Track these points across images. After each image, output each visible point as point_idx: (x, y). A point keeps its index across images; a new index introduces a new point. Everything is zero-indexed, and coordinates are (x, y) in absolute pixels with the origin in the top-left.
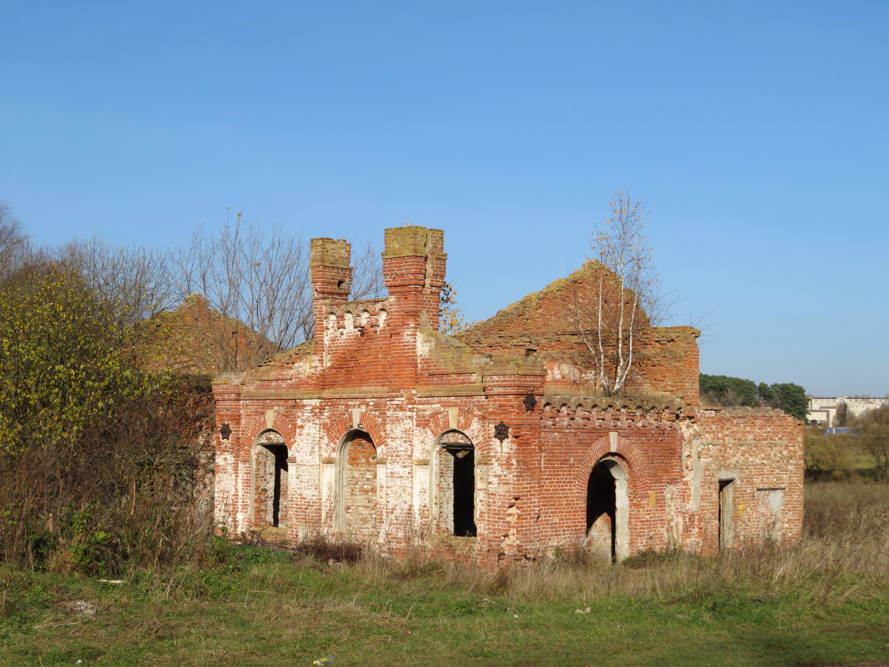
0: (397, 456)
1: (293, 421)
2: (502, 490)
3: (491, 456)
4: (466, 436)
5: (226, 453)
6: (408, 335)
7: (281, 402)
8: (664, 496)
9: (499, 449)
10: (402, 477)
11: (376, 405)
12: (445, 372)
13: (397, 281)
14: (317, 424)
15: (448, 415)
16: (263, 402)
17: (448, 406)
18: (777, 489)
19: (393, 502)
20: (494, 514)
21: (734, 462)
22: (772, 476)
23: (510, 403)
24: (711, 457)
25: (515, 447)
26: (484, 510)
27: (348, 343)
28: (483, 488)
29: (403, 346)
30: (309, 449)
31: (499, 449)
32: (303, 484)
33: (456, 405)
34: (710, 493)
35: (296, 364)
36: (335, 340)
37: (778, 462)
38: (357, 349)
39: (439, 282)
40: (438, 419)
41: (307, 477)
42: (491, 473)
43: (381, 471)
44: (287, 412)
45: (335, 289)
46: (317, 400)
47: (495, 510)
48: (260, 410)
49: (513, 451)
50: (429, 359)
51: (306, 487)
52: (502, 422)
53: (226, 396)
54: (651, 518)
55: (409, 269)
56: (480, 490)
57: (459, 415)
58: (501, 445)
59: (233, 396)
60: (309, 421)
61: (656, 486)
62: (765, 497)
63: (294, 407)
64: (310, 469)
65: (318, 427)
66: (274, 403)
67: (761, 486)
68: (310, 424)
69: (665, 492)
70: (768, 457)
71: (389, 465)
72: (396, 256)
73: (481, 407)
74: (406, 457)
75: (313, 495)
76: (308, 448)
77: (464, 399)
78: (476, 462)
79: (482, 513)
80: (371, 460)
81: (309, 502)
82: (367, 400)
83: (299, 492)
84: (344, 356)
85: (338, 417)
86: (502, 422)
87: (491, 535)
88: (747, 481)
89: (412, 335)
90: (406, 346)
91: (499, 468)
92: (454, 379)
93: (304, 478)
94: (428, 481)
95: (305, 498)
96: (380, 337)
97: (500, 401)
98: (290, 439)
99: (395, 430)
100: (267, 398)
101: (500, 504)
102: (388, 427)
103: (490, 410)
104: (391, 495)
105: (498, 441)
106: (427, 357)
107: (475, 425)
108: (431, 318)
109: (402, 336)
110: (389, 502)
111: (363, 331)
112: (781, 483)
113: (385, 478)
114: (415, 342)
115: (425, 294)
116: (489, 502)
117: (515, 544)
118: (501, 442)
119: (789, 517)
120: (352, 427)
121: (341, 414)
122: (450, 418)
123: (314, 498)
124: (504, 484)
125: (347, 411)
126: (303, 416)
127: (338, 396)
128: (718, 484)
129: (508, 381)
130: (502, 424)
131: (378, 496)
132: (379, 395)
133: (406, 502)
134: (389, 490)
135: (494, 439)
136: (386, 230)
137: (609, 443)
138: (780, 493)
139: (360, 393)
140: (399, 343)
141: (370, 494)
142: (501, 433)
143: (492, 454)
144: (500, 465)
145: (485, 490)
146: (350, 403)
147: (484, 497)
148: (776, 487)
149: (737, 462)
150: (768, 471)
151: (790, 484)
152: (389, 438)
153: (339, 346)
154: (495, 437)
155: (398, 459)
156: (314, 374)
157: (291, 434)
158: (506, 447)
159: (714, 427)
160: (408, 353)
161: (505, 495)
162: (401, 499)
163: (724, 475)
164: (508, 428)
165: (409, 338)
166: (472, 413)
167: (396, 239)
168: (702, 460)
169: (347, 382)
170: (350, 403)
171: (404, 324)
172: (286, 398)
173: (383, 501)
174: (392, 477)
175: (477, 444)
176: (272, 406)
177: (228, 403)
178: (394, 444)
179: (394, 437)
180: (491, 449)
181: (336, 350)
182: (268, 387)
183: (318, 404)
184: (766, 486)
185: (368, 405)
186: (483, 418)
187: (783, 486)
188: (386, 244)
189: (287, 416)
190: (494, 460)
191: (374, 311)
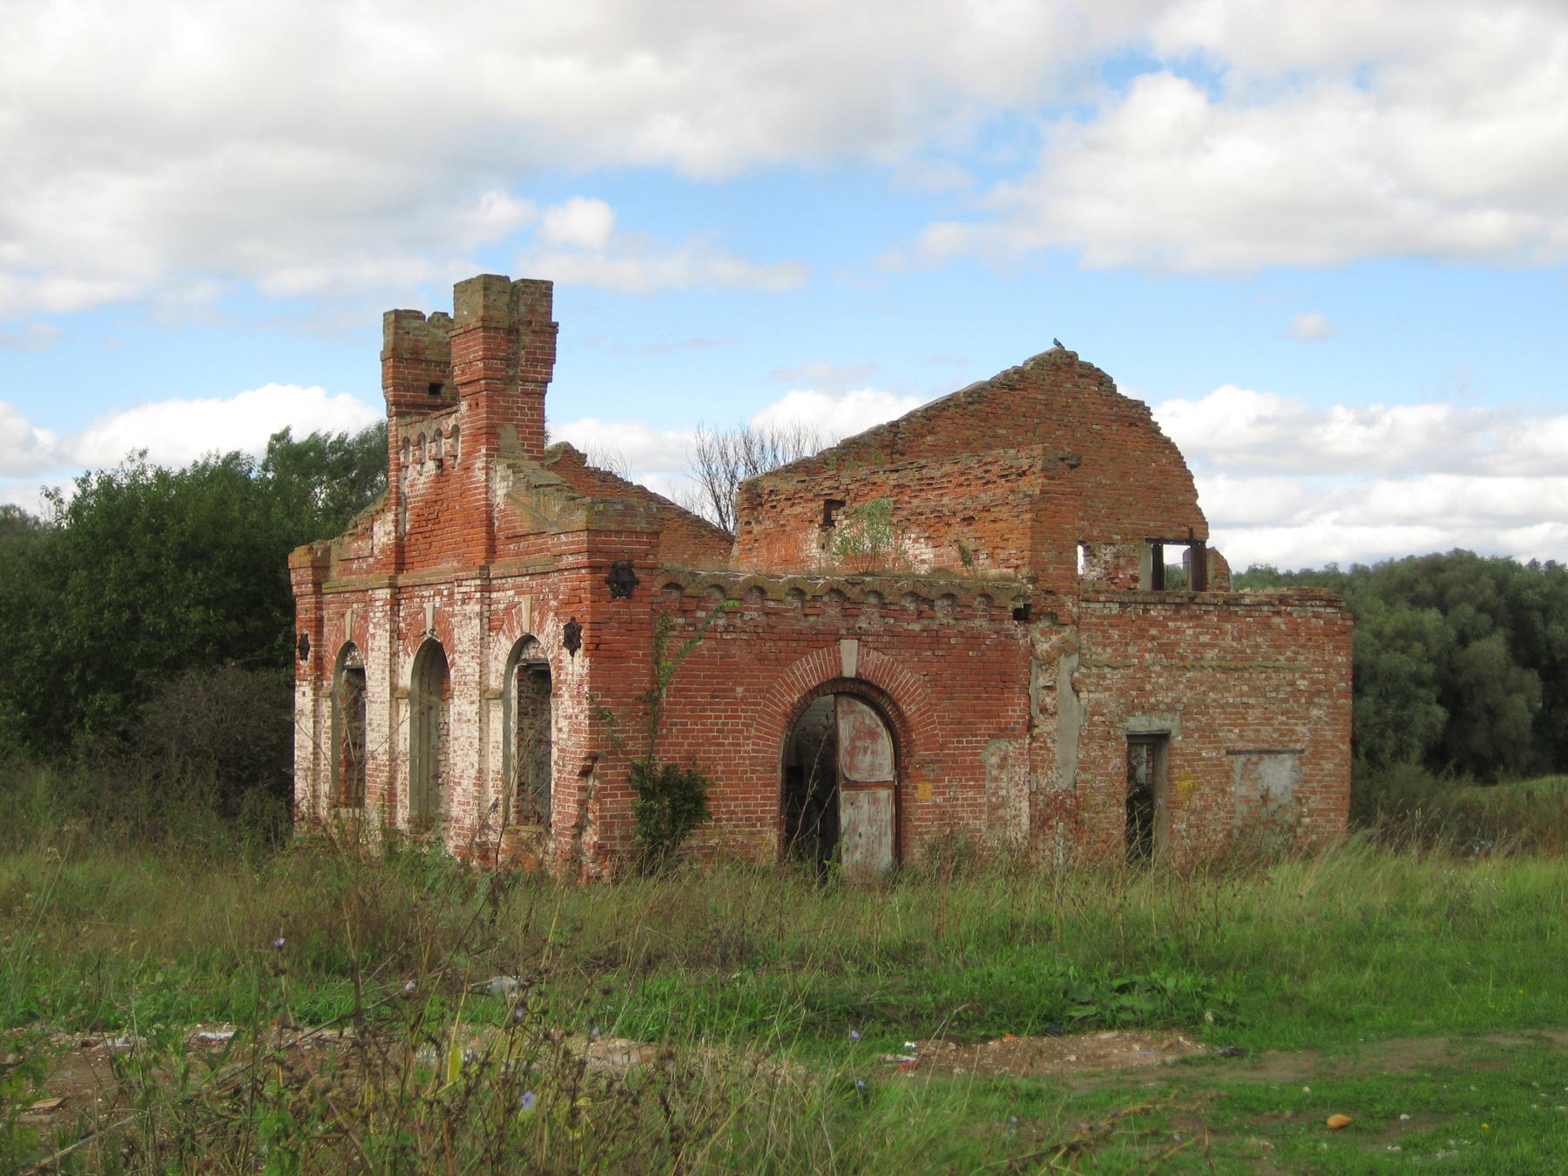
8: (980, 761)
18: (1280, 752)
21: (1168, 700)
22: (1270, 729)
34: (1104, 756)
37: (1286, 700)
39: (541, 373)
45: (423, 397)
61: (958, 742)
62: (1250, 767)
66: (353, 597)
67: (1239, 746)
69: (984, 755)
70: (1256, 690)
88: (1200, 737)
111: (440, 463)
112: (1291, 741)
115: (512, 396)
119: (1313, 805)
128: (1124, 739)
138: (1289, 761)
146: (426, 593)
148: (1279, 747)
150: (1257, 718)
151: (1315, 743)
159: (1115, 634)
163: (1140, 723)
168: (1083, 695)
184: (1251, 746)
187: (1298, 746)
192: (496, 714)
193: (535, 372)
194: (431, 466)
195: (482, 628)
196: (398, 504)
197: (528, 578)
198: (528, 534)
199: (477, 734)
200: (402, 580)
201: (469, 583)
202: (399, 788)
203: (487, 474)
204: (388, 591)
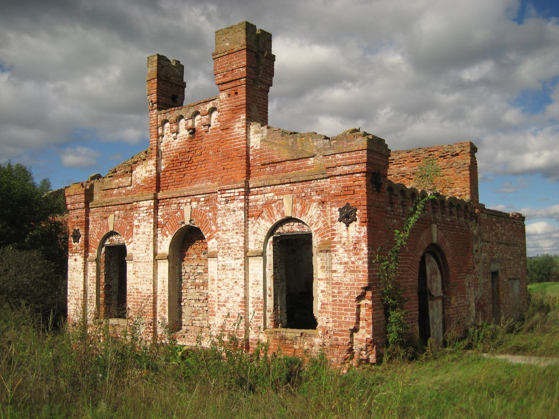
0: (229, 248)
1: (131, 222)
2: (349, 278)
3: (335, 242)
4: (304, 223)
5: (76, 254)
6: (239, 128)
10: (234, 269)
11: (207, 201)
12: (279, 159)
14: (151, 223)
17: (283, 194)
19: (224, 295)
20: (339, 305)
23: (357, 183)
24: (487, 252)
25: (364, 229)
26: (326, 302)
27: (180, 146)
29: (234, 139)
30: (143, 247)
31: (345, 234)
32: (139, 280)
35: (134, 172)
36: (168, 145)
38: (188, 150)
40: (272, 208)
41: (143, 273)
43: (212, 264)
44: (127, 215)
47: (341, 301)
49: (362, 234)
51: (142, 283)
52: (348, 204)
54: (458, 304)
55: (240, 62)
56: (322, 280)
57: (294, 202)
58: (347, 230)
59: (83, 205)
63: (131, 209)
64: (145, 264)
65: (152, 225)
68: (145, 224)
71: (220, 258)
72: (226, 53)
73: (320, 192)
74: (238, 248)
75: (148, 290)
77: (300, 185)
78: (315, 250)
79: (323, 304)
80: (202, 256)
81: (145, 296)
82: (199, 196)
83: (135, 286)
84: (175, 159)
86: (348, 204)
87: (337, 329)
89: (243, 127)
90: (238, 138)
91: (346, 255)
92: (290, 166)
93: (140, 274)
94: (262, 272)
95: (141, 293)
96: (211, 136)
97: (345, 181)
99: (226, 223)
100: (110, 204)
101: (347, 294)
102: (219, 220)
103: (332, 192)
104: (223, 288)
105: (343, 225)
106: (258, 147)
107: (314, 211)
108: (260, 114)
109: (233, 129)
110: (220, 295)
111: (193, 131)
113: (216, 271)
115: (256, 90)
116: (334, 293)
117: (365, 339)
118: (348, 226)
120: (183, 223)
121: (173, 212)
123: (149, 292)
126: (139, 216)
127: (170, 196)
129: (356, 158)
130: (348, 206)
131: (210, 289)
133: (238, 295)
134: (220, 282)
135: (338, 223)
136: (216, 32)
137: (431, 234)
139: (190, 190)
141: (202, 287)
143: (335, 240)
144: (346, 251)
145: (327, 279)
147: (326, 287)
149: (499, 256)
152: (220, 231)
153: (172, 150)
154: (340, 220)
155: (230, 252)
156: (149, 177)
157: (130, 234)
160: (240, 145)
161: (353, 284)
162: (233, 291)
163: (494, 267)
164: (356, 210)
165: (240, 130)
166: (310, 198)
169: (179, 183)
170: (182, 201)
173: (215, 294)
174: (224, 269)
175: (315, 231)
177: (78, 211)
178: (225, 237)
179: (225, 229)
181: (169, 154)
182: (112, 195)
183: (152, 204)
185: (198, 201)
188: (217, 44)
190: (338, 246)
192: (256, 265)
193: (266, 79)
194: (184, 133)
195: (245, 216)
196: (158, 155)
197: (288, 185)
199: (243, 277)
201: (229, 191)
202: (159, 309)
203: (246, 130)
204: (153, 201)
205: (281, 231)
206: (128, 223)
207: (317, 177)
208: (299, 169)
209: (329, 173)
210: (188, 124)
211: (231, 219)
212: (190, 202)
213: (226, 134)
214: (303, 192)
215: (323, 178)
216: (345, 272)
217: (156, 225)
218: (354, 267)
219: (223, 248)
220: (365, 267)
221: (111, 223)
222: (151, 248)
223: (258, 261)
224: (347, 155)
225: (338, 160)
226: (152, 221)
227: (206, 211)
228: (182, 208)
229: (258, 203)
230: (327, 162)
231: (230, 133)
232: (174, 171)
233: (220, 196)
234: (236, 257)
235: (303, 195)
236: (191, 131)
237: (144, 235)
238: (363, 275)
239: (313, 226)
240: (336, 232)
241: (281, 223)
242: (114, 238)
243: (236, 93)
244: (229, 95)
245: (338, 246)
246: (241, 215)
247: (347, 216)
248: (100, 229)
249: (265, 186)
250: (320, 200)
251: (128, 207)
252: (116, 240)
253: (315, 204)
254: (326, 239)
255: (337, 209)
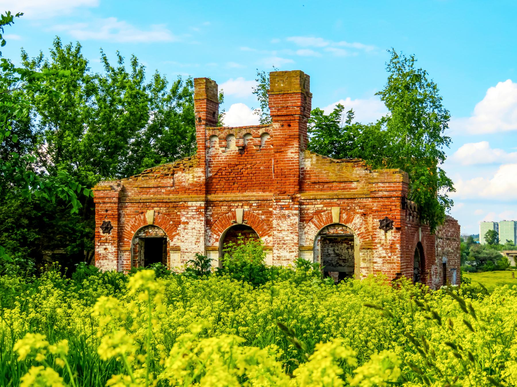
2: (386, 267)
3: (376, 243)
6: (292, 153)
7: (161, 205)
9: (383, 237)
10: (289, 260)
11: (258, 206)
13: (283, 111)
14: (202, 221)
15: (331, 213)
16: (146, 205)
23: (393, 204)
27: (229, 158)
28: (366, 266)
29: (287, 161)
30: (194, 240)
33: (339, 205)
38: (238, 163)
40: (321, 216)
42: (375, 255)
46: (202, 203)
48: (140, 211)
49: (397, 238)
50: (311, 171)
53: (107, 200)
55: (295, 103)
56: (363, 268)
58: (386, 235)
59: (115, 200)
60: (194, 218)
65: (203, 223)
66: (153, 205)
68: (195, 221)
71: (275, 251)
74: (293, 244)
76: (193, 238)
77: (346, 201)
82: (253, 202)
85: (221, 215)
86: (387, 218)
89: (296, 152)
91: (384, 251)
92: (337, 186)
97: (384, 202)
98: (172, 233)
99: (281, 225)
100: (148, 201)
103: (374, 208)
105: (383, 232)
107: (357, 220)
109: (287, 153)
111: (243, 149)
114: (299, 158)
118: (386, 232)
120: (235, 222)
121: (224, 213)
122: (333, 215)
124: (388, 263)
125: (230, 211)
126: (187, 214)
127: (221, 199)
129: (394, 187)
130: (387, 219)
132: (261, 198)
135: (378, 230)
140: (284, 158)
142: (386, 225)
143: (376, 241)
144: (384, 249)
152: (275, 230)
153: (220, 161)
154: (380, 228)
155: (285, 246)
156: (197, 182)
158: (392, 236)
160: (293, 166)
161: (390, 272)
165: (293, 155)
166: (354, 211)
167: (281, 80)
170: (233, 204)
171: (286, 144)
172: (168, 201)
176: (153, 207)
178: (280, 235)
179: (280, 229)
180: (375, 237)
181: (216, 164)
183: (203, 205)
185: (251, 206)
186: (364, 215)
189: (169, 215)
190: (378, 245)
191: (257, 134)
197: (336, 200)
198: (333, 182)
200: (211, 197)
201: (284, 201)
204: (204, 203)
205: (327, 232)
206: (171, 219)
207: (360, 196)
208: (344, 189)
209: (372, 195)
210: (238, 142)
211: (285, 222)
212: (242, 206)
213: (279, 156)
214: (348, 206)
215: (366, 198)
216: (383, 263)
217: (208, 223)
218: (390, 260)
219: (278, 244)
220: (398, 260)
221: (150, 216)
222: (201, 241)
223: (309, 254)
224: (387, 185)
225: (380, 187)
226: (203, 219)
227: (258, 214)
228: (233, 210)
229: (309, 211)
230: (372, 187)
231: (285, 156)
232: (222, 179)
233: (275, 204)
234: (291, 250)
235: (348, 208)
236: (241, 148)
237: (194, 230)
238: (398, 266)
239: (357, 230)
240: (377, 236)
241: (327, 227)
242: (150, 231)
243: (289, 126)
244: (282, 126)
245: (378, 245)
246: (297, 219)
247: (387, 226)
248: (135, 222)
249: (316, 199)
250: (363, 213)
251: (171, 205)
252: (153, 233)
253: (358, 215)
254: (367, 240)
255: (378, 220)
